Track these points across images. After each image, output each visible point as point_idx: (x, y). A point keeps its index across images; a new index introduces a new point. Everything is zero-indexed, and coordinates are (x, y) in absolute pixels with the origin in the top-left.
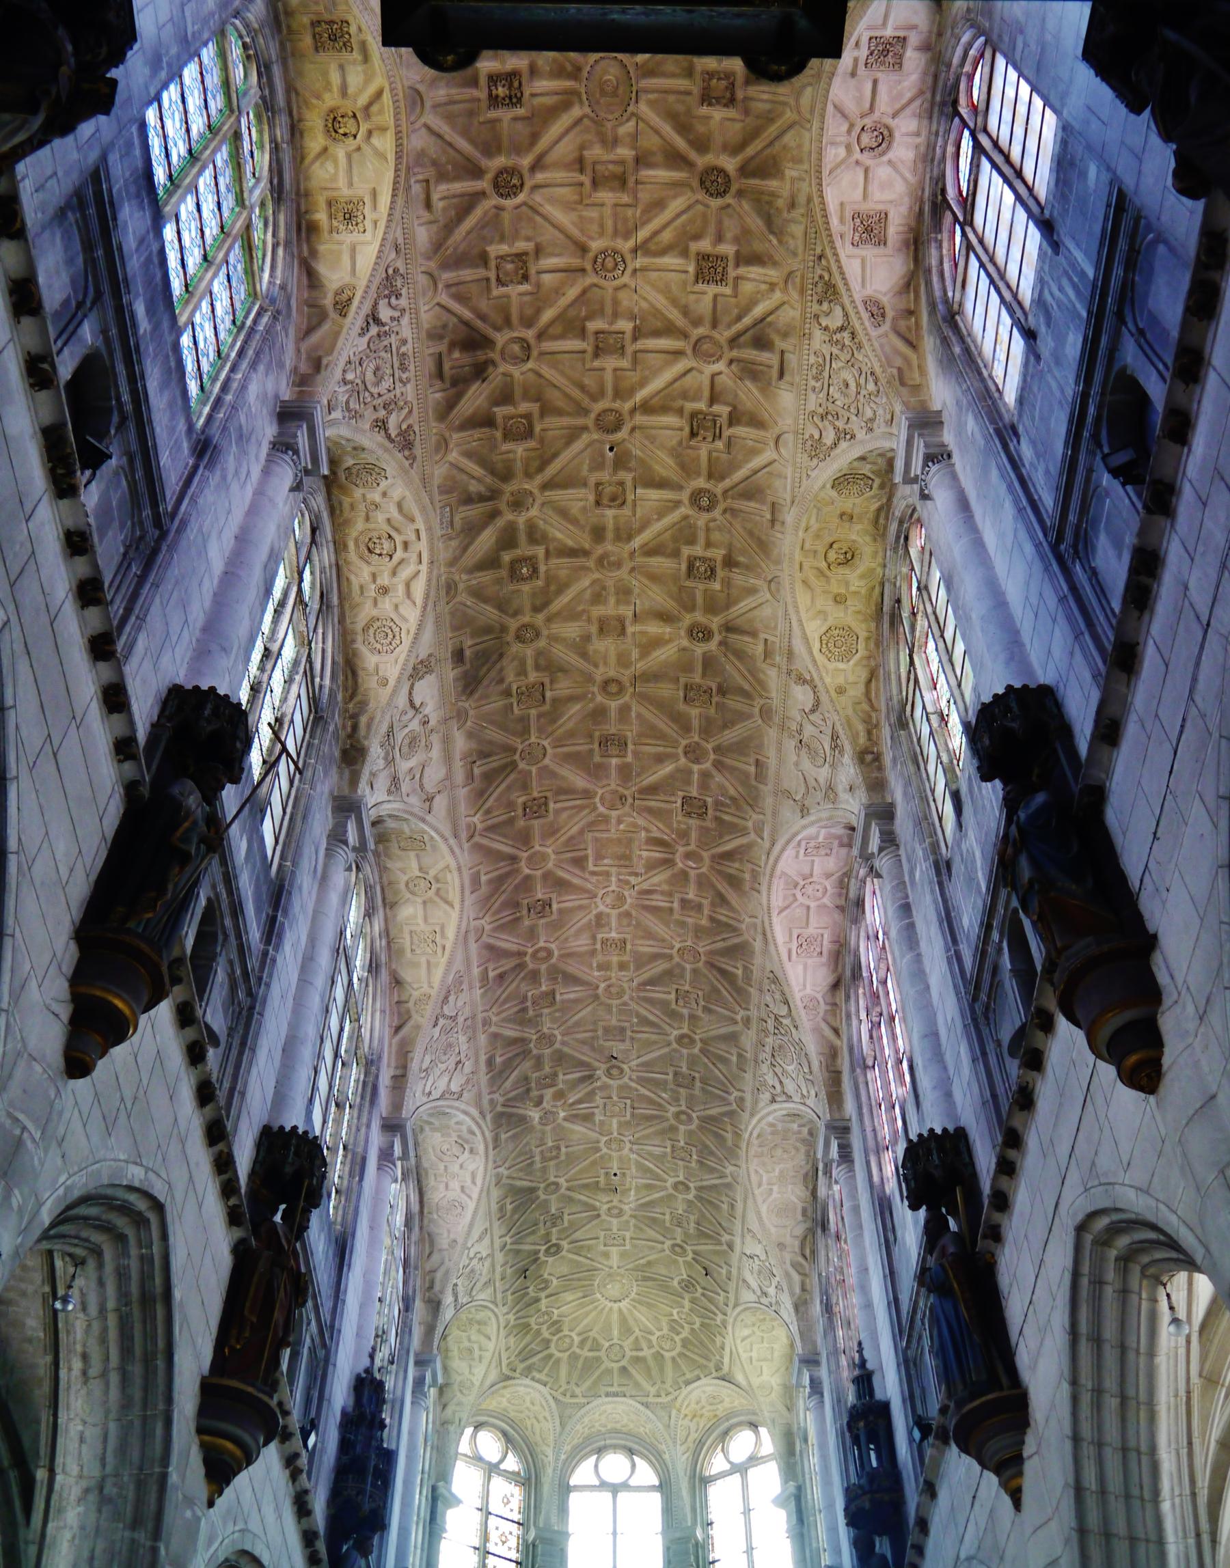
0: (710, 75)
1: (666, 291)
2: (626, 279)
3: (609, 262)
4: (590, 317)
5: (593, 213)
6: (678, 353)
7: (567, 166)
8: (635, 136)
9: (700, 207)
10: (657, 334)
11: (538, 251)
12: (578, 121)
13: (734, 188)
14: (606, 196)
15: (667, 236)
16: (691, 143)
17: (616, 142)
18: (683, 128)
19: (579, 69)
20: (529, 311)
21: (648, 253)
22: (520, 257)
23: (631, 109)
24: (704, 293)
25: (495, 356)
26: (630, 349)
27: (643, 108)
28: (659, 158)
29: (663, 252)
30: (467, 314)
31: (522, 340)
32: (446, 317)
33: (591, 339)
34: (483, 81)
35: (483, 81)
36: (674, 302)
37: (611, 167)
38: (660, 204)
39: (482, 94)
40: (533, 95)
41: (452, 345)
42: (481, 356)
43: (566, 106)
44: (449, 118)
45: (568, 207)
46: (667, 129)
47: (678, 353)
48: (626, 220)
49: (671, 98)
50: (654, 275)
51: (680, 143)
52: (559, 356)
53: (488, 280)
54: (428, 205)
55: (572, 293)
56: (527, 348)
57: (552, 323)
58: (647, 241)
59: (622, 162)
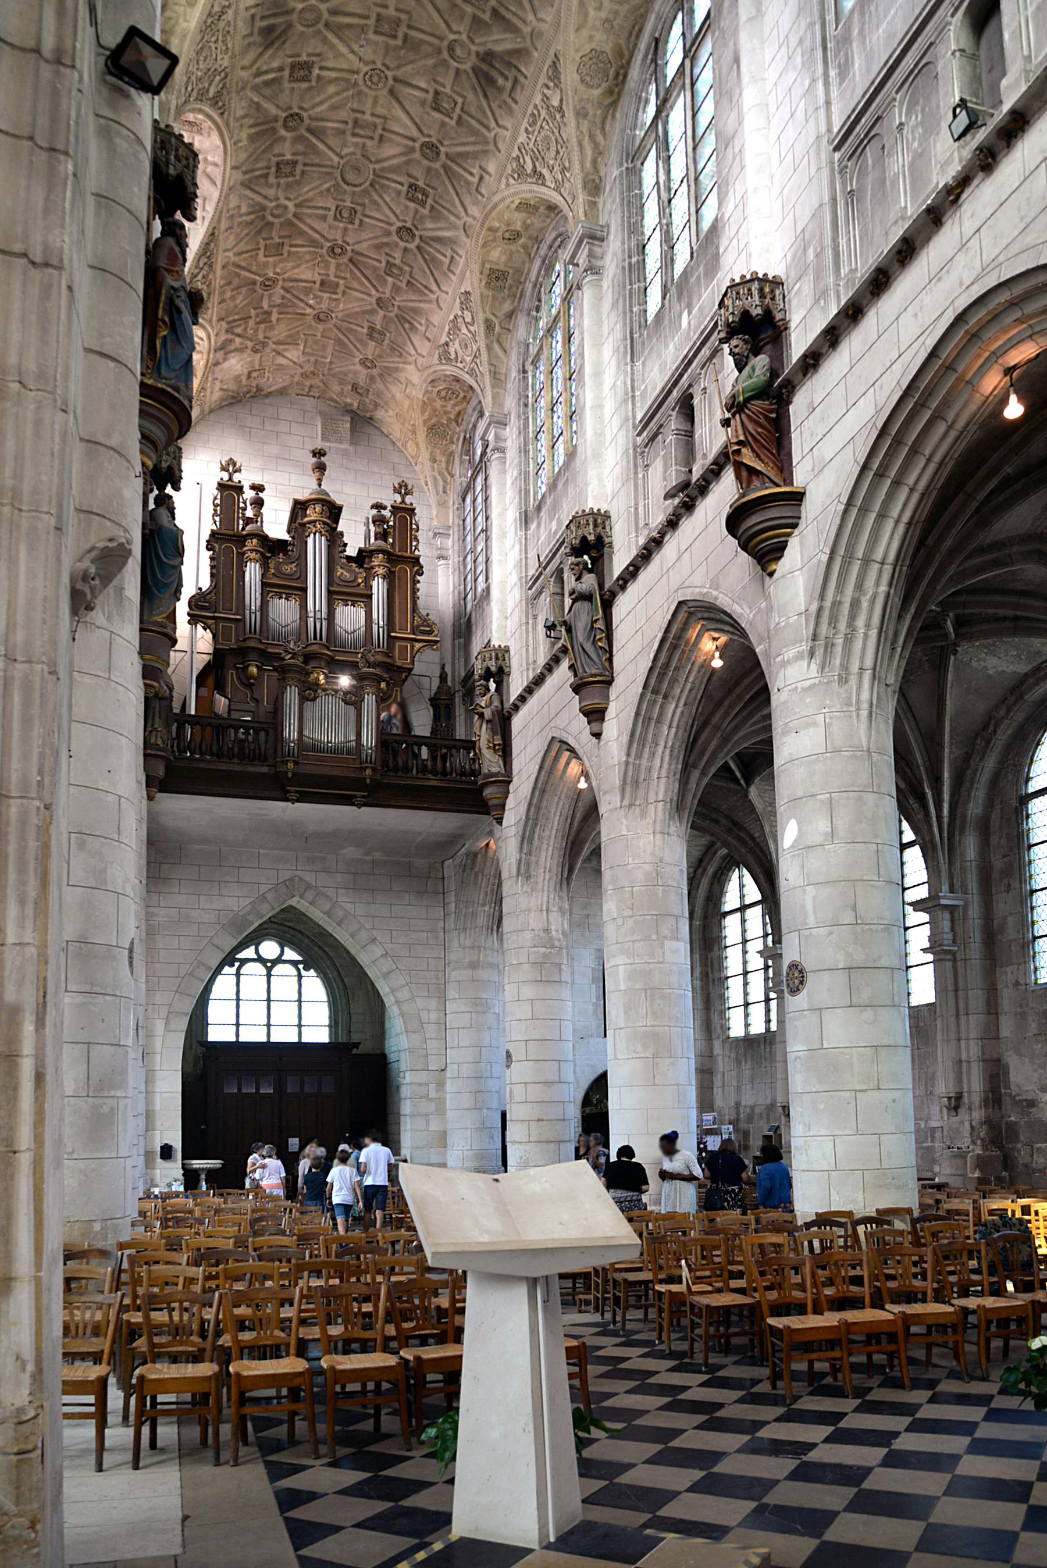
0: (292, 174)
1: (338, 55)
2: (366, 69)
3: (375, 76)
4: (398, 48)
5: (379, 110)
6: (334, 12)
7: (391, 141)
8: (344, 145)
9: (305, 106)
10: (350, 26)
11: (423, 103)
12: (377, 162)
13: (281, 121)
14: (367, 117)
15: (332, 89)
16: (307, 139)
17: (356, 145)
18: (313, 147)
19: (371, 185)
20: (441, 70)
21: (347, 81)
22: (437, 108)
23: (342, 162)
24: (309, 55)
25: (474, 59)
26: (372, 21)
27: (336, 159)
28: (329, 132)
29: (336, 79)
30: (484, 102)
31: (451, 56)
32: (497, 112)
33: (400, 35)
34: (428, 206)
35: (428, 206)
36: (332, 47)
37: (362, 133)
38: (333, 108)
39: (430, 201)
40: (402, 184)
41: (500, 90)
42: (484, 67)
43: (383, 169)
44: (453, 205)
45: (398, 120)
46: (321, 146)
47: (334, 12)
48: (359, 102)
49: (317, 161)
50: (344, 66)
51: (315, 141)
52: (429, 30)
53: (462, 110)
54: (481, 178)
55: (408, 68)
56: (451, 49)
57: (427, 56)
58: (348, 89)
59: (354, 135)
